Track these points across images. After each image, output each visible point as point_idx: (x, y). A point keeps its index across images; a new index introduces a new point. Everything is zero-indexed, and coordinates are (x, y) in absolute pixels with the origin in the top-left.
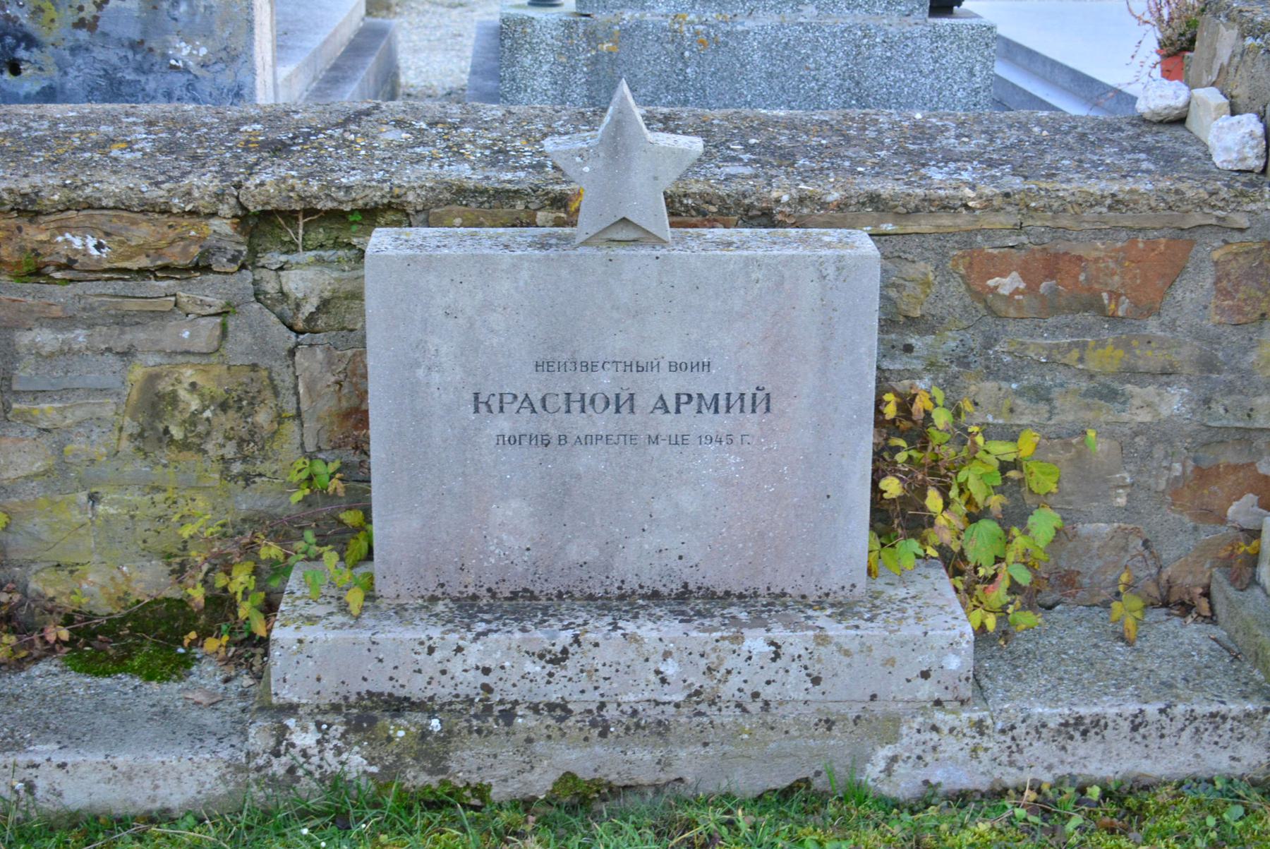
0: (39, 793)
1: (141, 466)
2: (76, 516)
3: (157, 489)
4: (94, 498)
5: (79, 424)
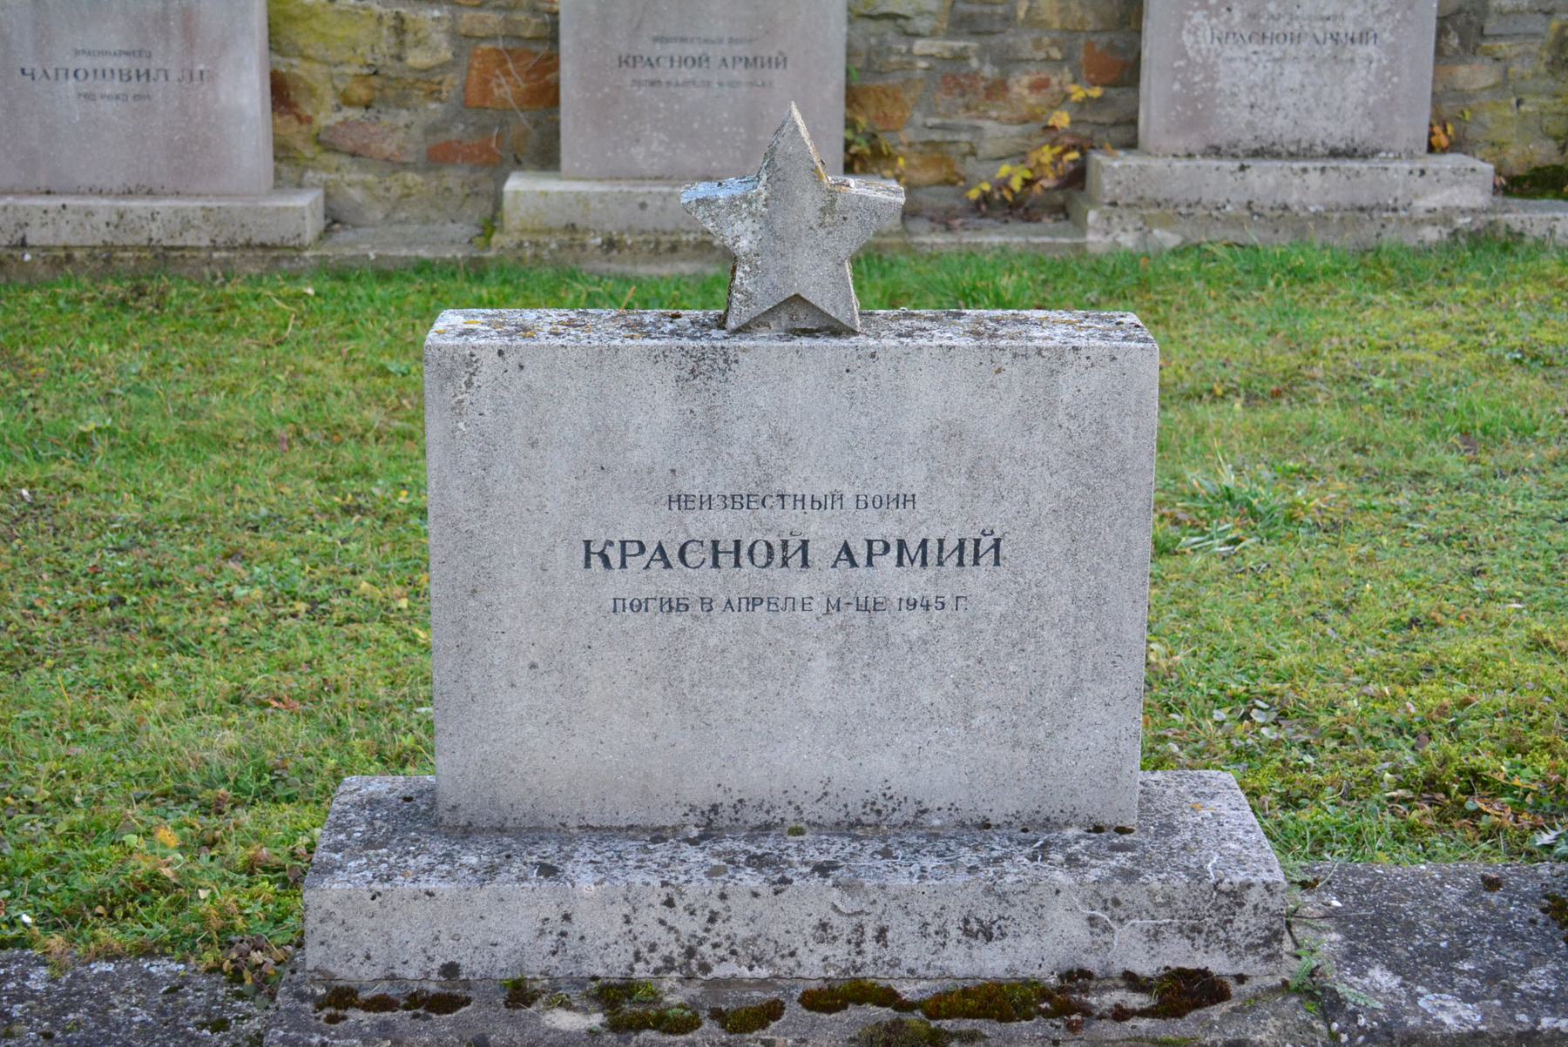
0: (1557, 237)
1: (1550, 82)
2: (1509, 113)
3: (1557, 96)
4: (1519, 103)
5: (1518, 55)
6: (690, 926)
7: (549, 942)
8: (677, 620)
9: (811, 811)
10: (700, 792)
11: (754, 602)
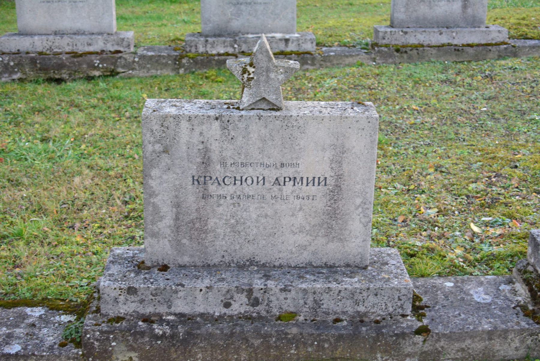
6: (50, 44)
7: (31, 46)
8: (49, 4)
9: (69, 32)
10: (54, 29)
11: (59, 1)
